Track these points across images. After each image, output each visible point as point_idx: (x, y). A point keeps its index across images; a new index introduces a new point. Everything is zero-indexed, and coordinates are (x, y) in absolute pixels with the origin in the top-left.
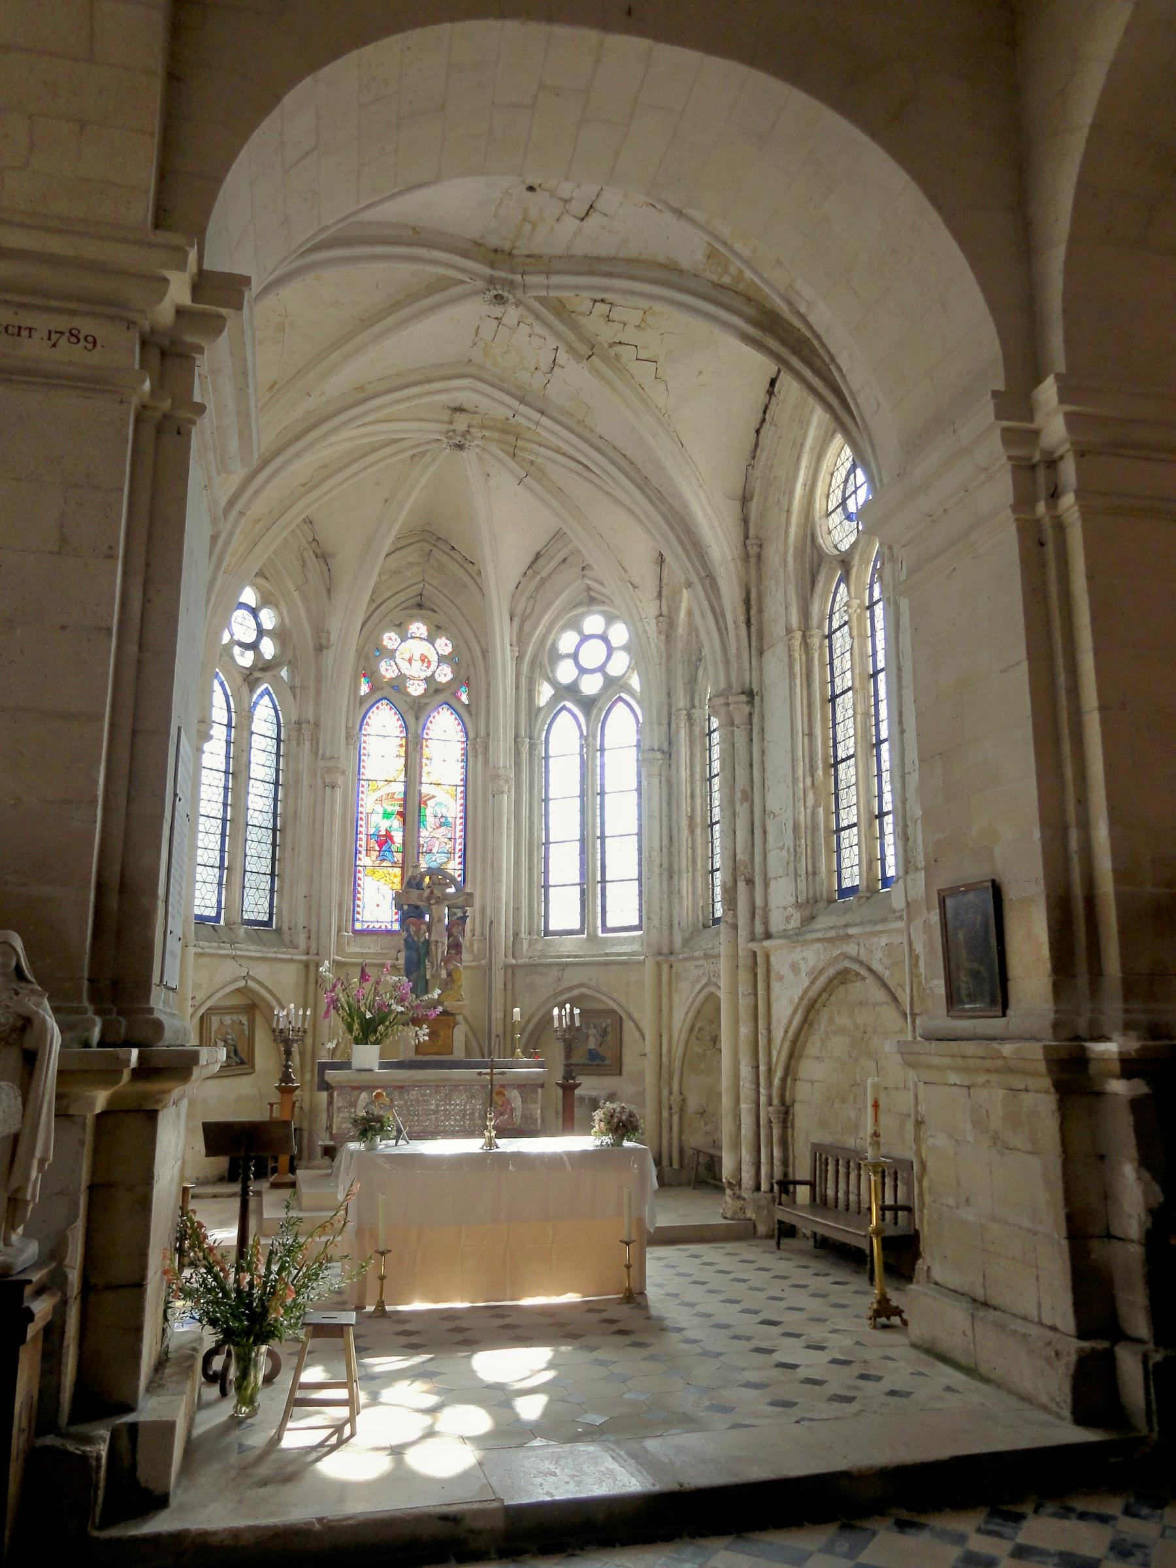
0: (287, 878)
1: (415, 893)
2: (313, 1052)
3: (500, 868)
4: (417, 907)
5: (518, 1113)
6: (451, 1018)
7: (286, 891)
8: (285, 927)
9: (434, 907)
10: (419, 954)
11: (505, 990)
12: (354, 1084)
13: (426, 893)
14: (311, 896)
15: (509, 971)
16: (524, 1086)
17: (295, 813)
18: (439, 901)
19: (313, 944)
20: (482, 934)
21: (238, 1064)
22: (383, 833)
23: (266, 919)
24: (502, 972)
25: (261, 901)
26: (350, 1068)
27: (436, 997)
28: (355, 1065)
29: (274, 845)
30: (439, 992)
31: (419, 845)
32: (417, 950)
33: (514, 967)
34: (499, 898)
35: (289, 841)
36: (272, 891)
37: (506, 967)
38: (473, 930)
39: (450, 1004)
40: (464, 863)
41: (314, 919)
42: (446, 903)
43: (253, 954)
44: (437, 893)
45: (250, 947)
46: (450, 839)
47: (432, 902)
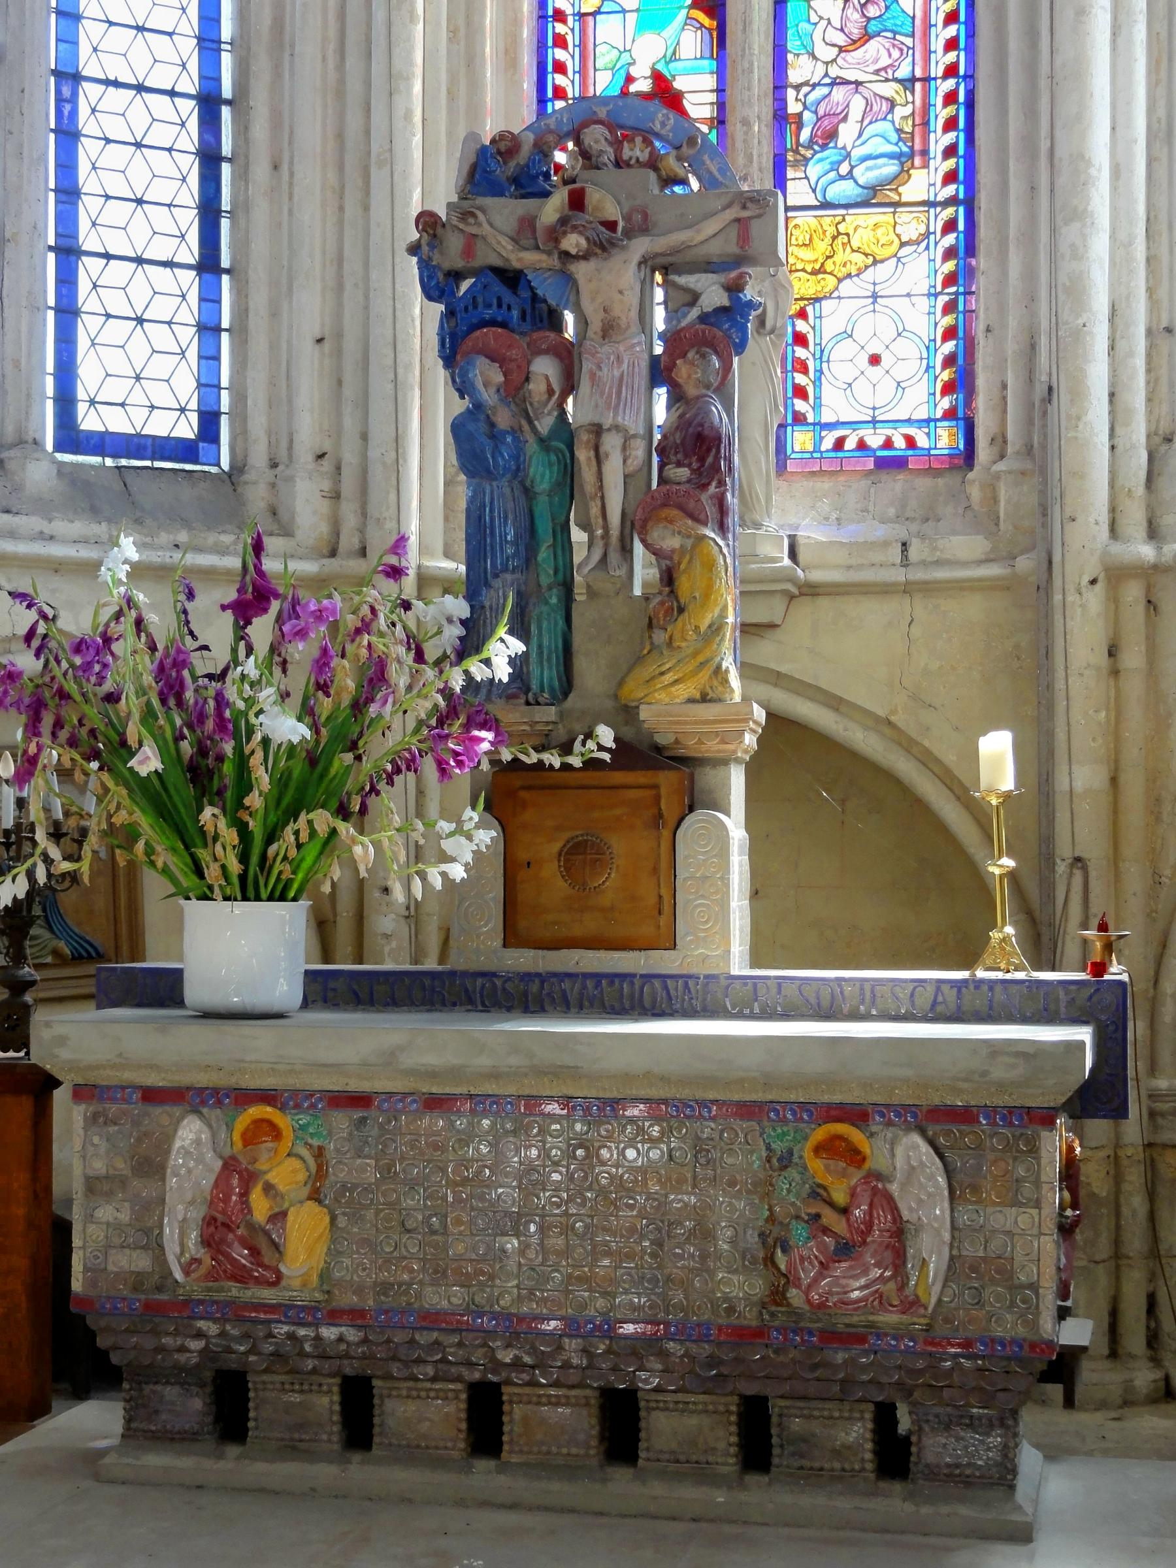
0: (258, 274)
1: (502, 212)
2: (360, 918)
3: (1081, 159)
4: (512, 278)
5: (931, 1254)
6: (667, 780)
7: (258, 324)
8: (258, 458)
9: (581, 270)
10: (528, 492)
11: (1115, 672)
12: (153, 1080)
13: (552, 208)
14: (339, 335)
15: (1133, 592)
16: (965, 1115)
17: (278, 25)
18: (606, 240)
19: (350, 520)
20: (1029, 450)
21: (61, 960)
22: (643, 85)
23: (187, 429)
24: (1095, 599)
25: (160, 366)
26: (179, 1002)
27: (503, 672)
28: (196, 992)
29: (210, 159)
30: (517, 646)
31: (781, 117)
32: (518, 471)
33: (1151, 575)
34: (1077, 291)
35: (260, 130)
36: (208, 329)
37: (1115, 575)
38: (1000, 441)
39: (666, 708)
40: (965, 176)
41: (350, 423)
42: (641, 246)
43: (57, 551)
44: (605, 203)
45: (60, 526)
46: (908, 83)
47: (573, 242)
